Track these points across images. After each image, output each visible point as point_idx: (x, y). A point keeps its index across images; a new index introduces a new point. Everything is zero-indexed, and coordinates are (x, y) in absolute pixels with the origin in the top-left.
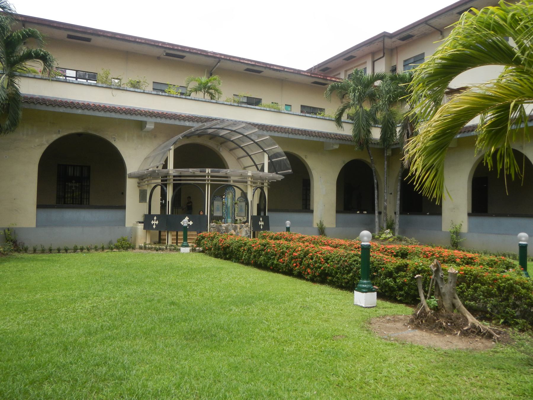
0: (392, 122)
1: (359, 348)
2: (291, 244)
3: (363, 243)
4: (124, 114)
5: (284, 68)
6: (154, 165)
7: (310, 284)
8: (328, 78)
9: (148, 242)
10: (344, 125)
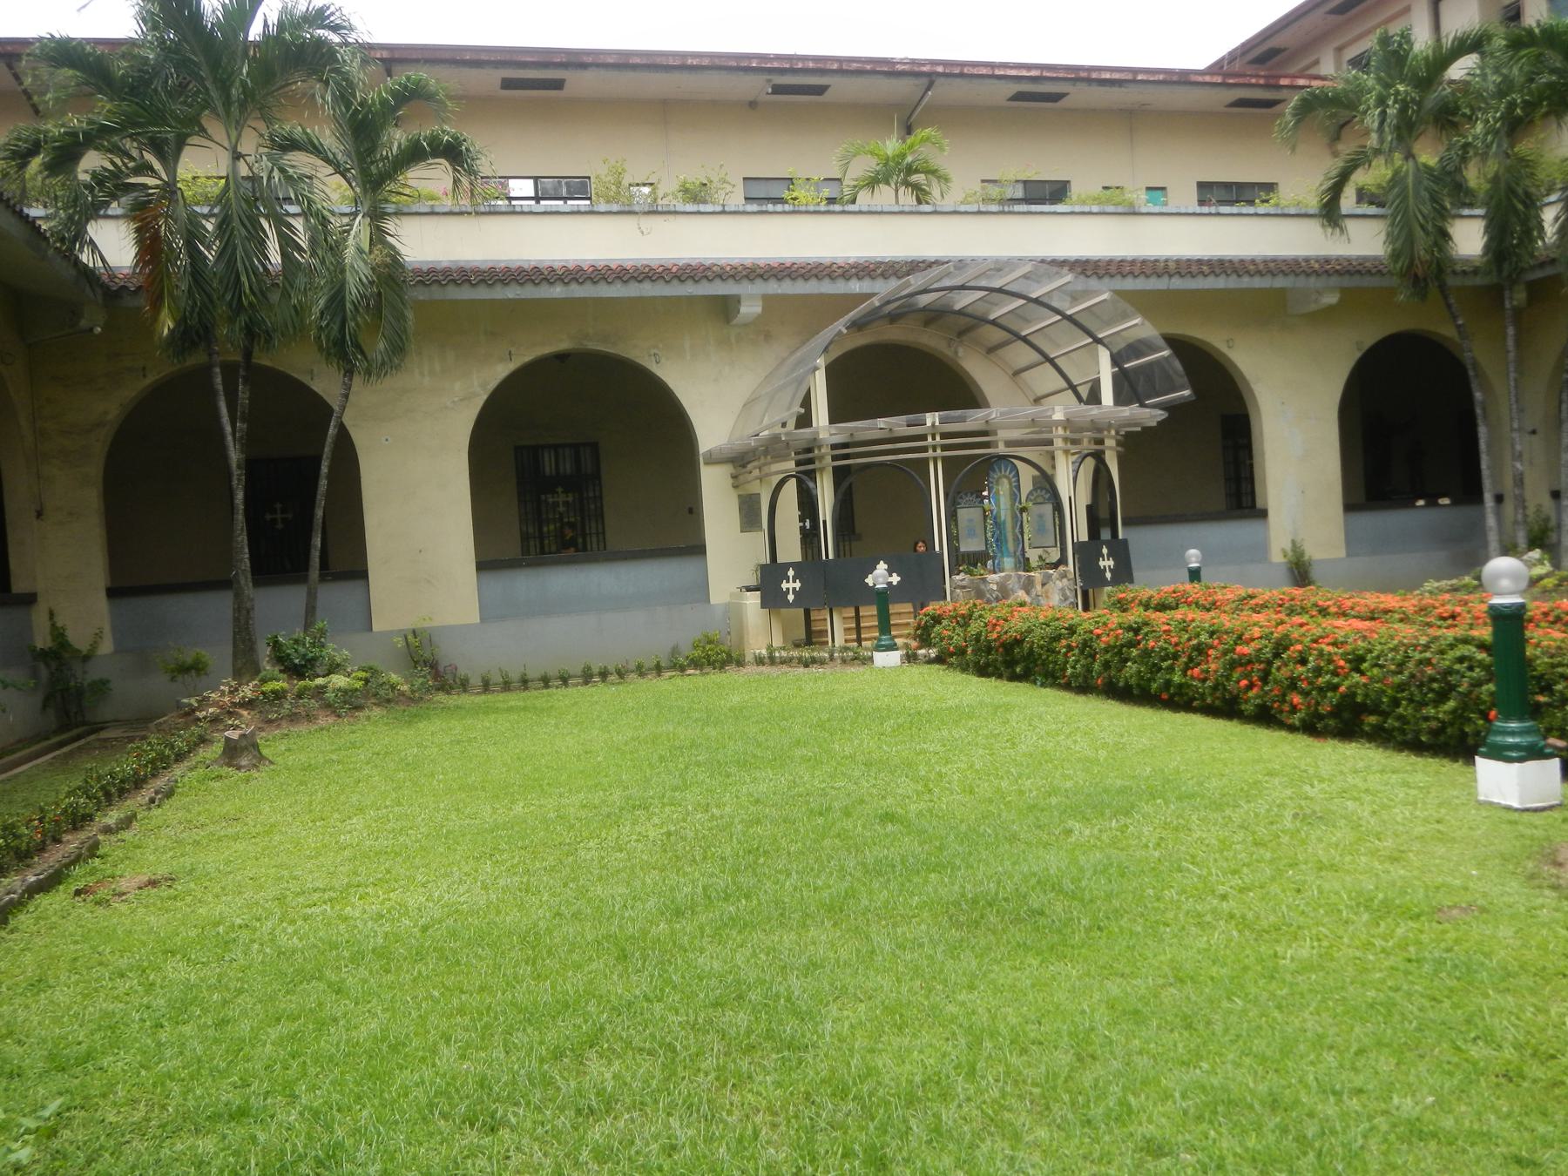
0: (1527, 194)
1: (1543, 947)
2: (1226, 621)
3: (1496, 601)
4: (675, 282)
6: (774, 419)
7: (1302, 741)
8: (1284, 82)
9: (778, 642)
10: (1351, 225)
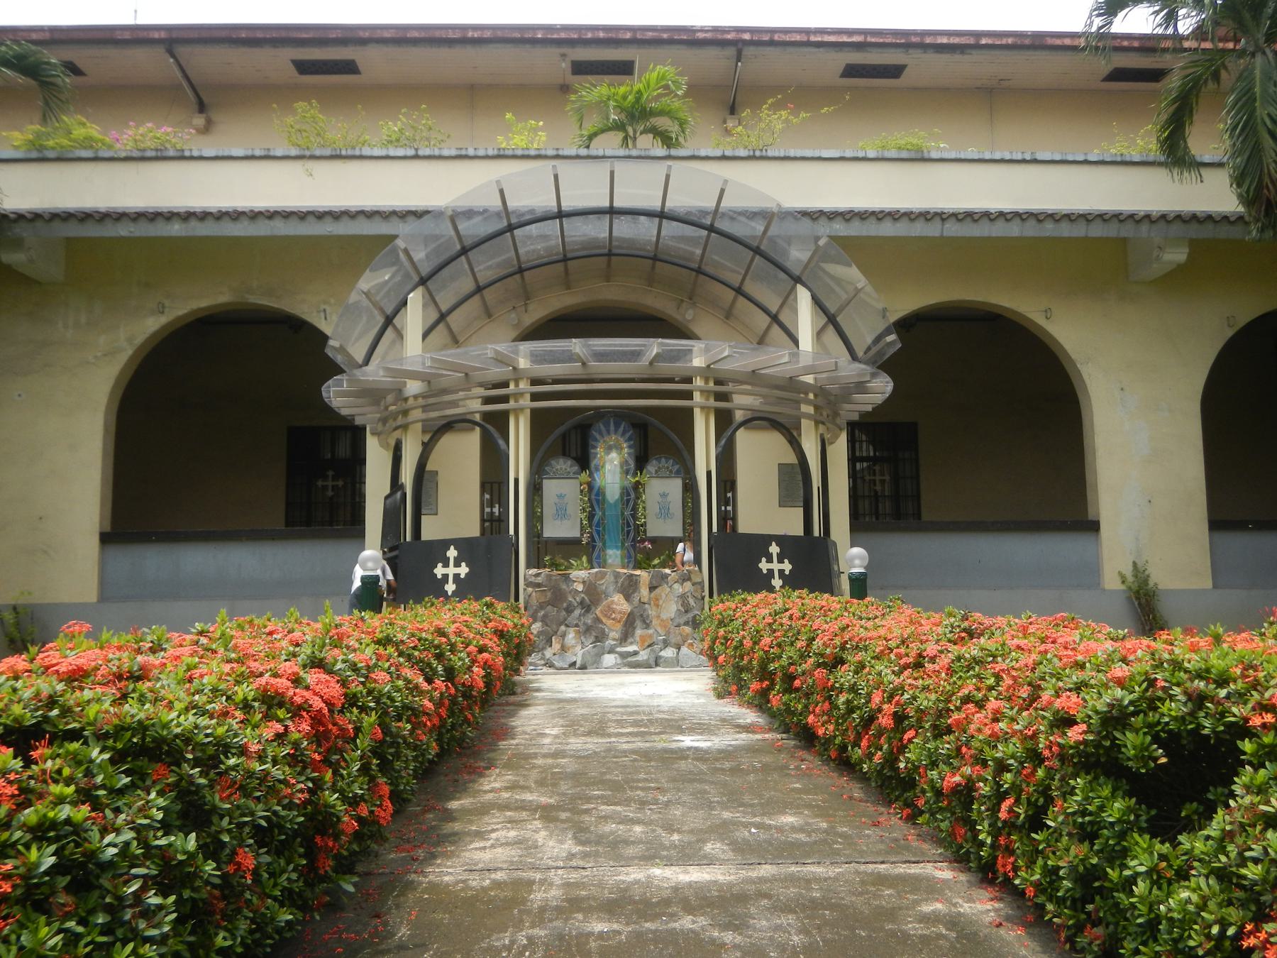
5: (978, 34)
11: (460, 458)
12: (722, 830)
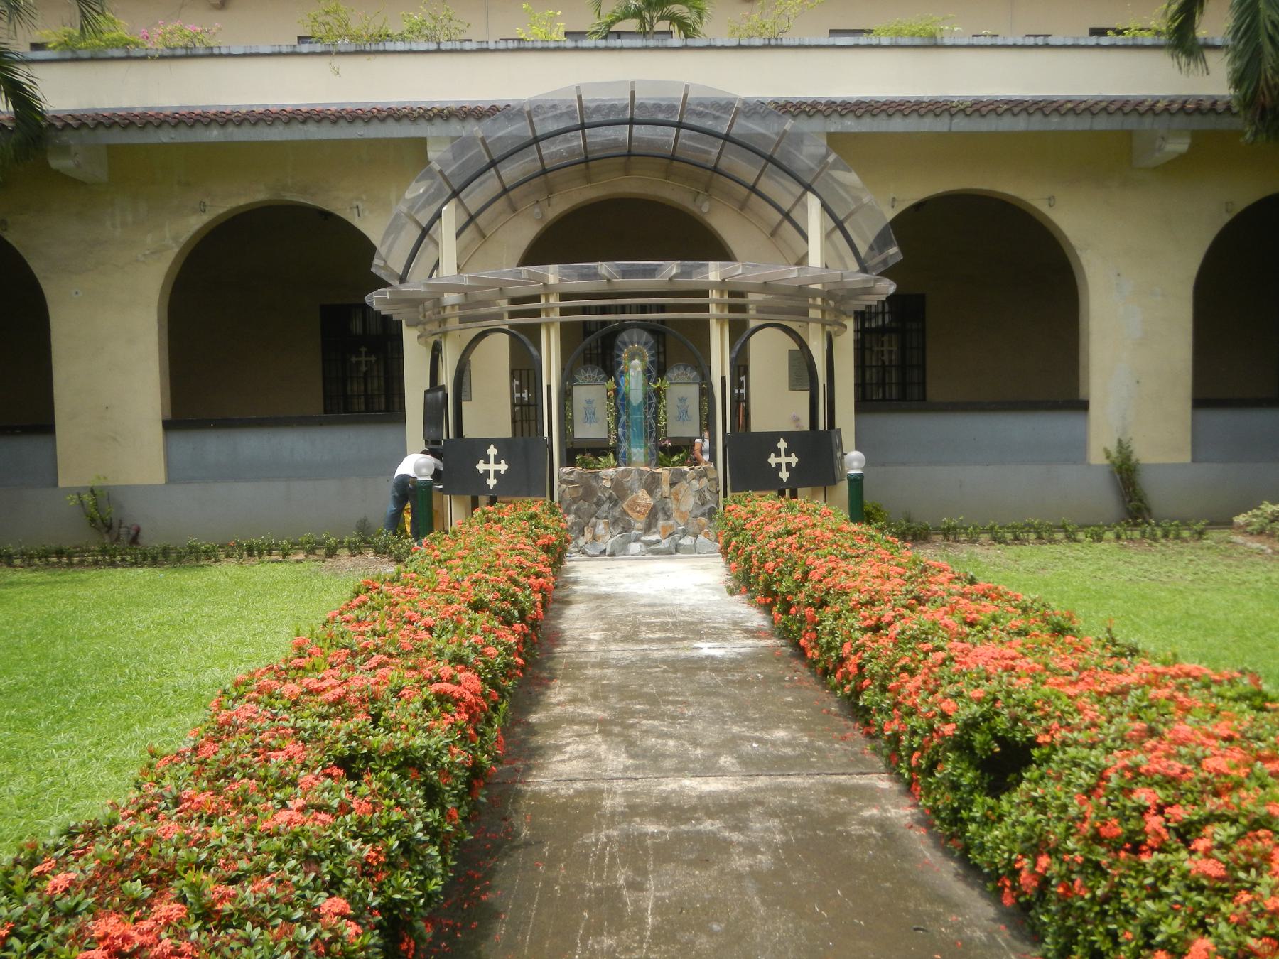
11: (495, 358)
12: (731, 744)
